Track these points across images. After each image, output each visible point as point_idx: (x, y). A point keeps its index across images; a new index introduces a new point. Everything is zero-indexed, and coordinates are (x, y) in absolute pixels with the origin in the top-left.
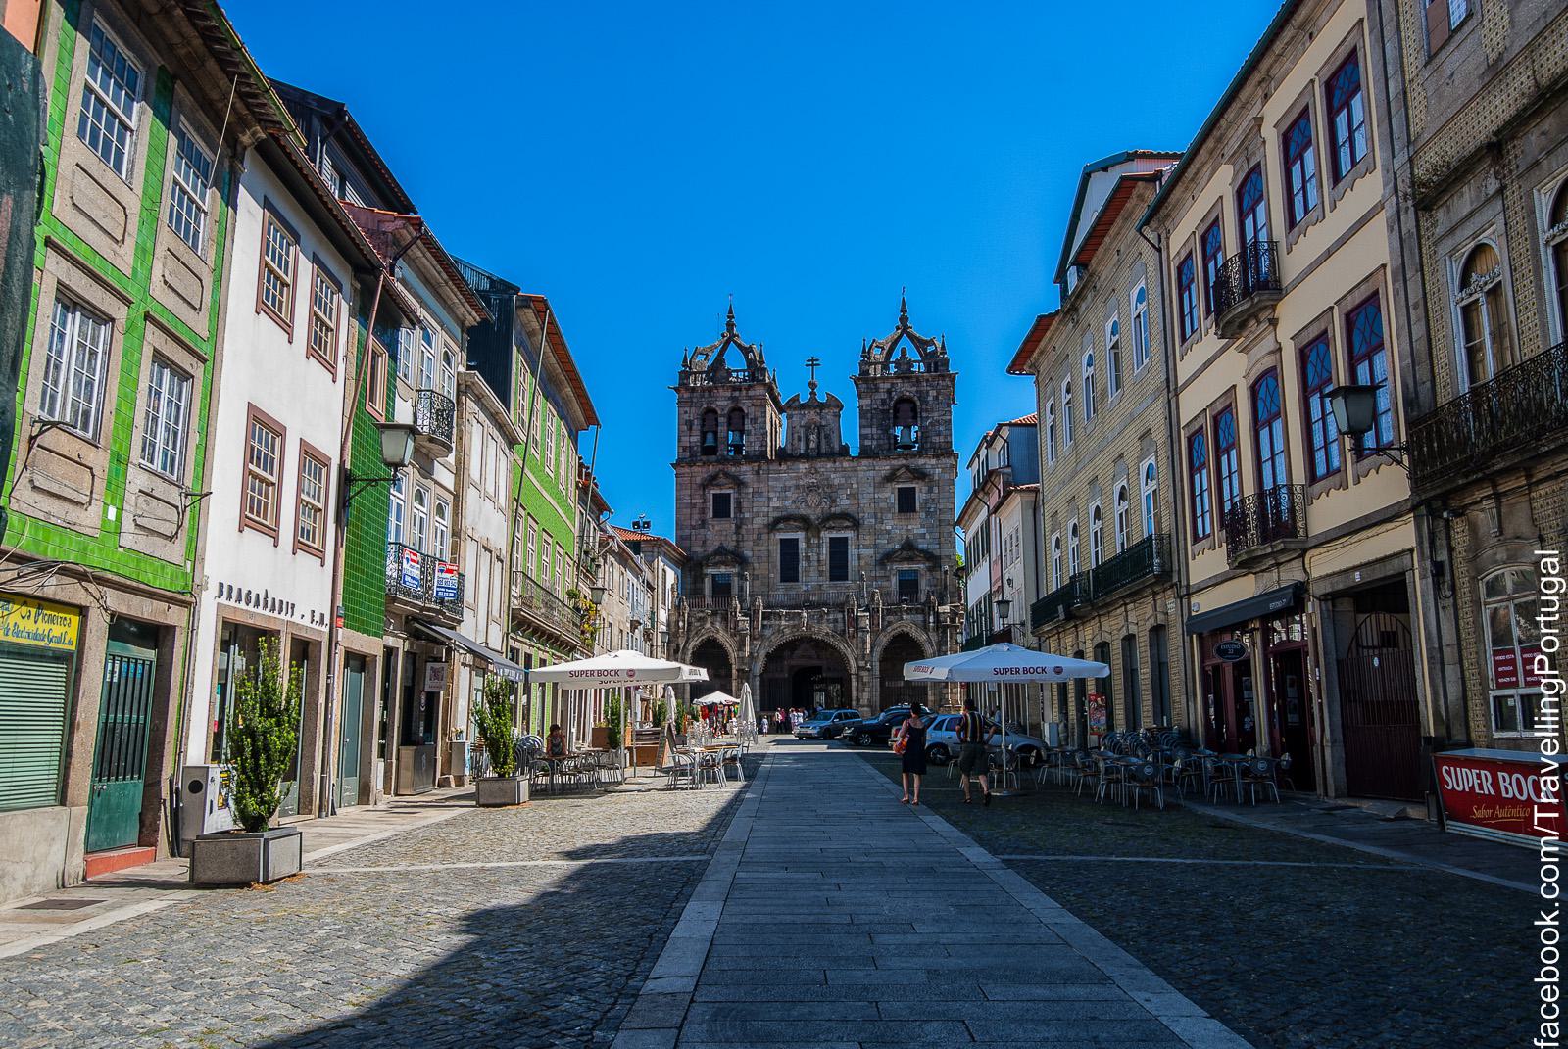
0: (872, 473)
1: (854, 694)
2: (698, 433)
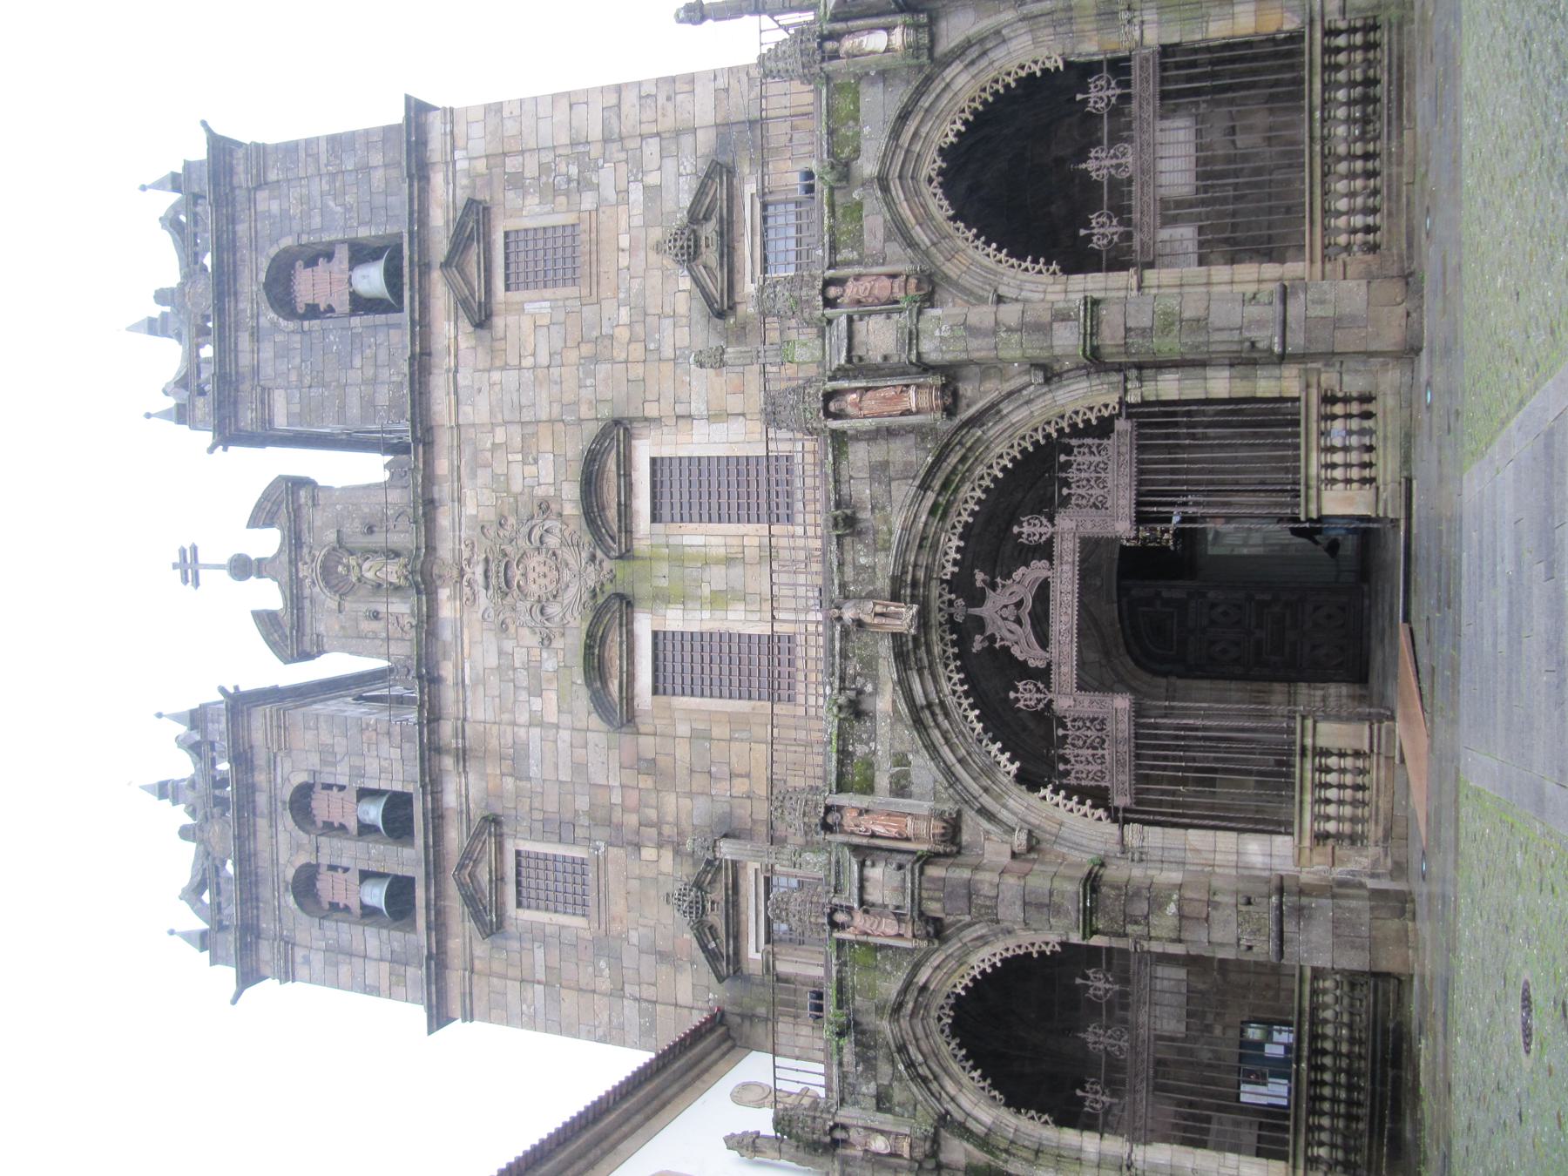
1: (1220, 384)
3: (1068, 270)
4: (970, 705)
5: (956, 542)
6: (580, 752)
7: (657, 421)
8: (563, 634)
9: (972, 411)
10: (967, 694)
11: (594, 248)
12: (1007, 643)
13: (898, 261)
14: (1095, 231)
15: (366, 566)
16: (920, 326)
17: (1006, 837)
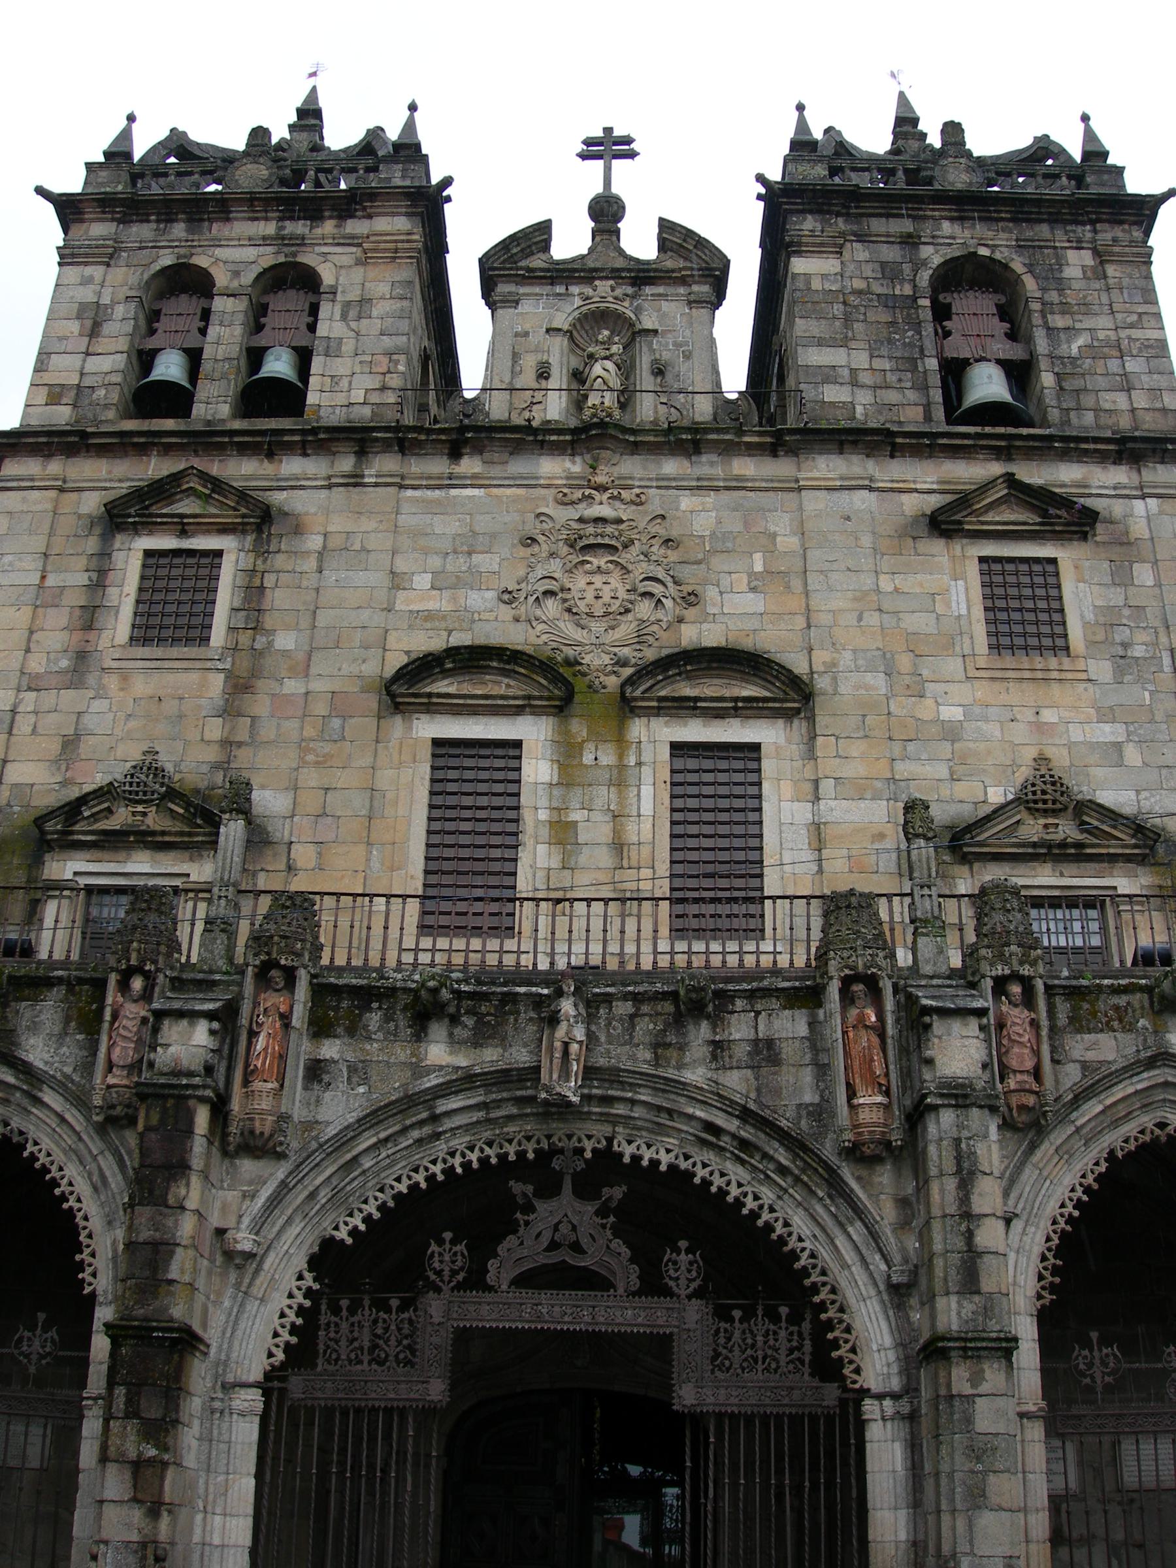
0: (862, 500)
2: (123, 344)
3: (1044, 1318)
4: (434, 1175)
5: (665, 1159)
6: (358, 635)
7: (810, 754)
8: (517, 620)
9: (854, 1184)
10: (449, 1171)
11: (1039, 675)
12: (522, 1230)
13: (1057, 1081)
14: (1096, 1353)
15: (609, 365)
16: (975, 1111)
17: (246, 1221)
